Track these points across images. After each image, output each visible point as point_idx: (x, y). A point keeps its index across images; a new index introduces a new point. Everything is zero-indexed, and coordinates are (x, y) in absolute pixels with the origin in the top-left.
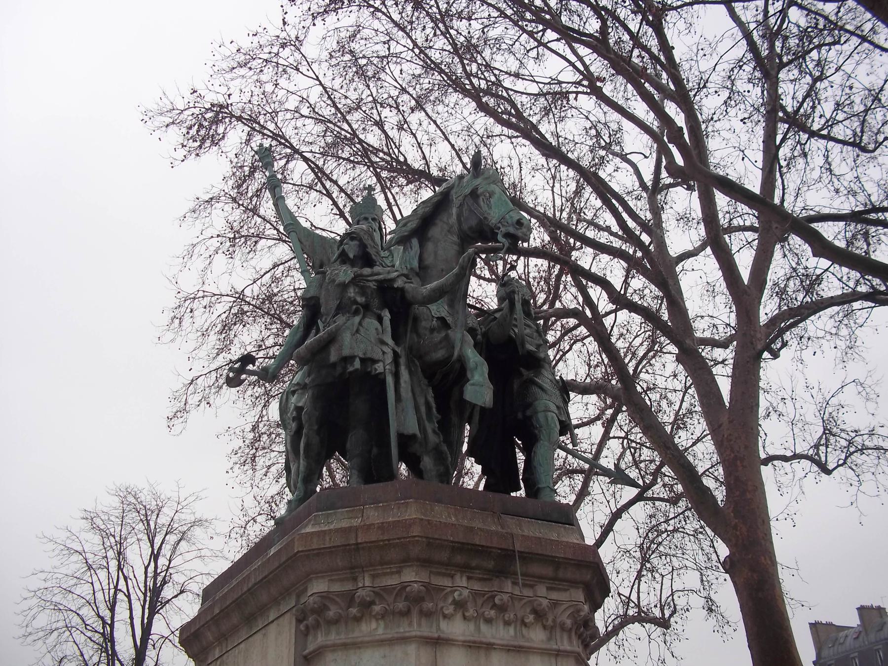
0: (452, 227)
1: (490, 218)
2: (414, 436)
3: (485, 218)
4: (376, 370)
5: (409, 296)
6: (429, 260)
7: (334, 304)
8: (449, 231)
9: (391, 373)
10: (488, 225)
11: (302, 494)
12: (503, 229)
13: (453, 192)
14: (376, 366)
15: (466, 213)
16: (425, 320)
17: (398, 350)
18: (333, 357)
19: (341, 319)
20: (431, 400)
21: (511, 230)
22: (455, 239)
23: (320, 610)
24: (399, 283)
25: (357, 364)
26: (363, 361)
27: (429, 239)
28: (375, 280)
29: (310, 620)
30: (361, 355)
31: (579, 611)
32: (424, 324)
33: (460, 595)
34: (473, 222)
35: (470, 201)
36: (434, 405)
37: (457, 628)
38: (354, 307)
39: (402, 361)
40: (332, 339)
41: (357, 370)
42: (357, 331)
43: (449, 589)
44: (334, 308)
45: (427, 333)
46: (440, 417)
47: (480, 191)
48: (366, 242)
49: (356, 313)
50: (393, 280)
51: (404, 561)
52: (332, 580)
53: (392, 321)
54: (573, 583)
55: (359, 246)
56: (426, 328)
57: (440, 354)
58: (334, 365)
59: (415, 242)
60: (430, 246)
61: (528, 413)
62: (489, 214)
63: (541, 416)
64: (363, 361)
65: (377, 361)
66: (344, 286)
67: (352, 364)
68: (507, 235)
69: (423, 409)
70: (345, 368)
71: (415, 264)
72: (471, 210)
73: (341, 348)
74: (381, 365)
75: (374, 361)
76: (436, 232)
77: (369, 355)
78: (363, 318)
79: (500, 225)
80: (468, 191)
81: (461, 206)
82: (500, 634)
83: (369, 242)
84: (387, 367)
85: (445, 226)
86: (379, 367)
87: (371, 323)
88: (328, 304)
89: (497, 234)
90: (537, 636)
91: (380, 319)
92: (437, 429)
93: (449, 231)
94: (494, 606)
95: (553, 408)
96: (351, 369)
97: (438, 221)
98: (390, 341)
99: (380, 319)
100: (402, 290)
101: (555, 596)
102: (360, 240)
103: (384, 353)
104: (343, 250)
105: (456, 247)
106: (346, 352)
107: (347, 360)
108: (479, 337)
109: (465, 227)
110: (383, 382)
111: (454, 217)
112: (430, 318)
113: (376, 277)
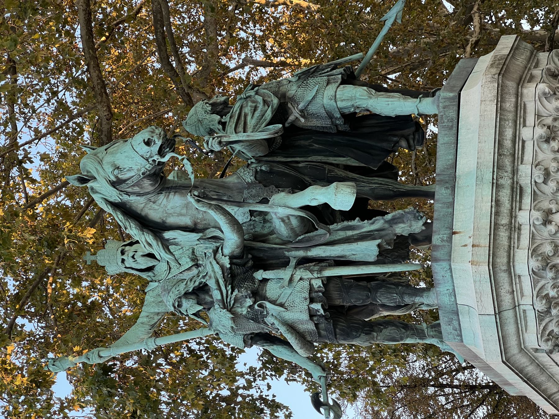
1: (142, 171)
2: (379, 246)
3: (143, 174)
4: (320, 287)
5: (237, 251)
6: (187, 221)
9: (320, 271)
12: (156, 158)
14: (316, 287)
15: (136, 189)
16: (254, 227)
17: (293, 262)
18: (311, 326)
20: (340, 225)
21: (155, 148)
22: (162, 197)
24: (226, 262)
25: (317, 306)
26: (312, 300)
27: (164, 222)
31: (545, 94)
32: (258, 229)
33: (538, 219)
35: (123, 187)
36: (346, 223)
38: (256, 307)
39: (301, 254)
40: (292, 327)
41: (322, 306)
42: (282, 305)
43: (532, 228)
44: (257, 325)
46: (358, 218)
47: (113, 178)
48: (183, 292)
50: (222, 267)
51: (510, 273)
52: (526, 330)
53: (266, 268)
54: (518, 95)
55: (186, 298)
56: (263, 227)
58: (316, 325)
59: (168, 235)
60: (172, 220)
62: (139, 170)
63: (340, 104)
64: (312, 300)
65: (311, 285)
66: (236, 317)
67: (317, 311)
68: (161, 153)
69: (350, 233)
70: (321, 316)
71: (194, 236)
74: (314, 282)
75: (311, 289)
77: (307, 296)
78: (265, 298)
81: (127, 193)
83: (182, 288)
84: (316, 275)
85: (148, 206)
86: (317, 283)
87: (271, 290)
88: (254, 327)
92: (370, 222)
93: (154, 203)
94: (545, 182)
95: (330, 91)
96: (322, 312)
97: (143, 214)
99: (265, 281)
100: (232, 258)
101: (531, 119)
102: (180, 298)
103: (301, 279)
105: (171, 195)
106: (305, 316)
107: (312, 315)
108: (263, 168)
109: (150, 189)
110: (329, 278)
111: (139, 198)
112: (252, 223)
113: (223, 288)
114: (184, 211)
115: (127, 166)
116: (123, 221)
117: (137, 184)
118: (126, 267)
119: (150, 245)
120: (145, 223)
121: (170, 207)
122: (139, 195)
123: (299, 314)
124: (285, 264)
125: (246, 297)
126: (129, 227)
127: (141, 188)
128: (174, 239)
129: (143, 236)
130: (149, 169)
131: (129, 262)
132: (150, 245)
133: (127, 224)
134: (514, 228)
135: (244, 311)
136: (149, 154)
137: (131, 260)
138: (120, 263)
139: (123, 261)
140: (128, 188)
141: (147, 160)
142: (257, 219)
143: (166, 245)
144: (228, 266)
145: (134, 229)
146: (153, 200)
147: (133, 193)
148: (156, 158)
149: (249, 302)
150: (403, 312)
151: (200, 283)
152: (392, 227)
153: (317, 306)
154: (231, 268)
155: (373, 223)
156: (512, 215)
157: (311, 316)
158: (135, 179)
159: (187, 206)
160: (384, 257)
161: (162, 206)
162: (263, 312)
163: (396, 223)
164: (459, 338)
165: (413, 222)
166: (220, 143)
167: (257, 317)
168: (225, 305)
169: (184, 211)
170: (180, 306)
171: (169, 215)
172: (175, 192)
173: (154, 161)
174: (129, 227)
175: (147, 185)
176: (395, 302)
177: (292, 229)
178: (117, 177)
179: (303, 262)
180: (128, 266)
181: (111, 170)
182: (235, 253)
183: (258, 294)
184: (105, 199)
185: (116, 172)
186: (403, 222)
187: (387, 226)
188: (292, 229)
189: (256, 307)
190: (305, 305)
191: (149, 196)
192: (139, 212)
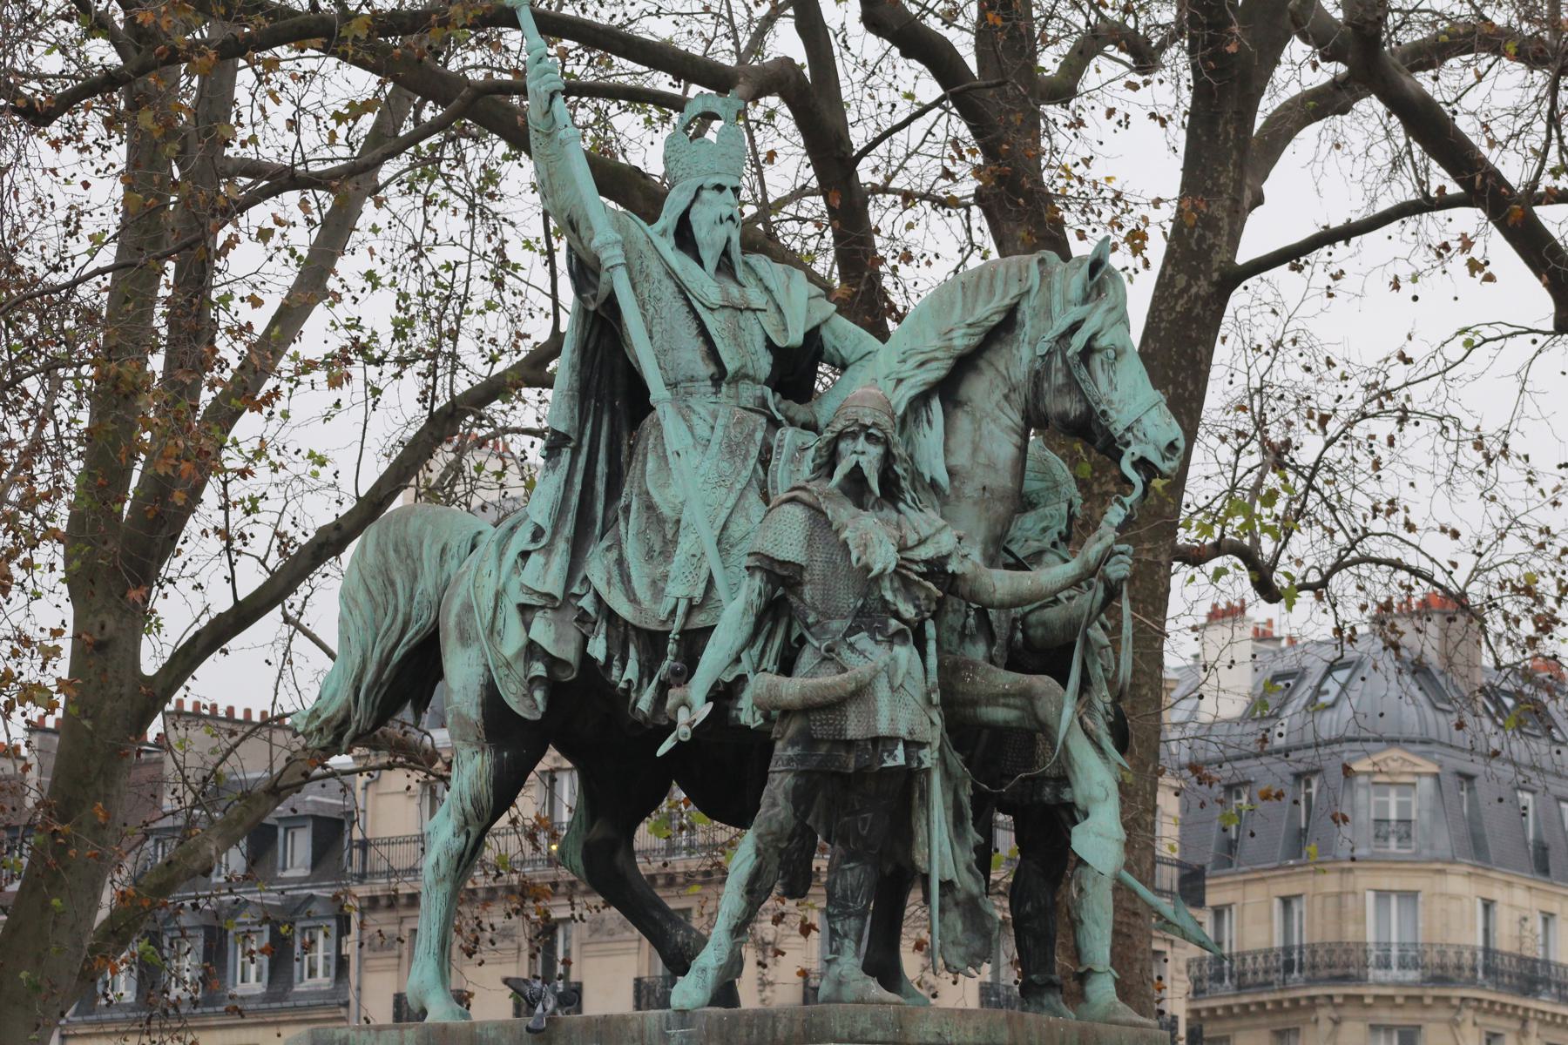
0: (1013, 389)
1: (1112, 413)
3: (1104, 413)
4: (920, 762)
6: (961, 459)
7: (849, 601)
8: (1006, 397)
10: (1106, 430)
11: (725, 958)
12: (1136, 450)
13: (1024, 306)
16: (955, 611)
18: (854, 729)
19: (862, 640)
20: (966, 800)
21: (1154, 457)
22: (1017, 418)
26: (907, 744)
28: (926, 562)
30: (908, 738)
34: (1073, 408)
36: (970, 814)
40: (861, 692)
45: (955, 639)
47: (1102, 342)
48: (895, 451)
49: (900, 635)
50: (949, 556)
56: (952, 629)
57: (999, 714)
58: (850, 744)
59: (936, 404)
61: (1067, 796)
62: (1110, 402)
67: (891, 754)
68: (1142, 464)
69: (950, 819)
72: (1069, 374)
73: (873, 713)
76: (982, 390)
77: (917, 737)
79: (1129, 436)
80: (1078, 342)
85: (999, 381)
89: (1121, 454)
91: (921, 645)
96: (890, 763)
97: (982, 364)
99: (921, 645)
102: (887, 443)
103: (932, 723)
104: (857, 467)
105: (1016, 439)
106: (883, 728)
107: (883, 743)
114: (982, 459)
115: (1118, 379)
116: (987, 324)
117: (1072, 385)
118: (701, 188)
119: (922, 364)
120: (965, 364)
122: (1038, 379)
125: (917, 606)
126: (971, 331)
127: (1059, 390)
128: (929, 422)
129: (947, 354)
130: (1111, 429)
132: (922, 364)
133: (977, 330)
135: (889, 596)
136: (1140, 435)
137: (726, 212)
138: (717, 180)
139: (720, 188)
140: (1065, 361)
141: (1129, 429)
142: (971, 621)
143: (920, 401)
144: (950, 569)
145: (966, 341)
146: (1013, 396)
147: (1048, 367)
148: (1136, 450)
149: (908, 611)
150: (475, 801)
151: (901, 491)
152: (957, 904)
153: (901, 761)
154: (946, 572)
155: (969, 869)
157: (876, 740)
158: (1087, 387)
159: (991, 466)
161: (997, 412)
162: (881, 634)
163: (964, 916)
164: (845, 1035)
165: (962, 950)
166: (1121, 580)
169: (982, 459)
170: (870, 438)
171: (977, 423)
172: (1019, 448)
173: (1128, 444)
174: (971, 331)
176: (844, 897)
177: (975, 703)
178: (1100, 351)
180: (705, 195)
181: (1118, 344)
182: (960, 583)
184: (1028, 292)
185: (1112, 354)
186: (964, 930)
187: (961, 896)
188: (975, 703)
189: (894, 623)
190: (903, 733)
191: (1026, 389)
192: (987, 355)
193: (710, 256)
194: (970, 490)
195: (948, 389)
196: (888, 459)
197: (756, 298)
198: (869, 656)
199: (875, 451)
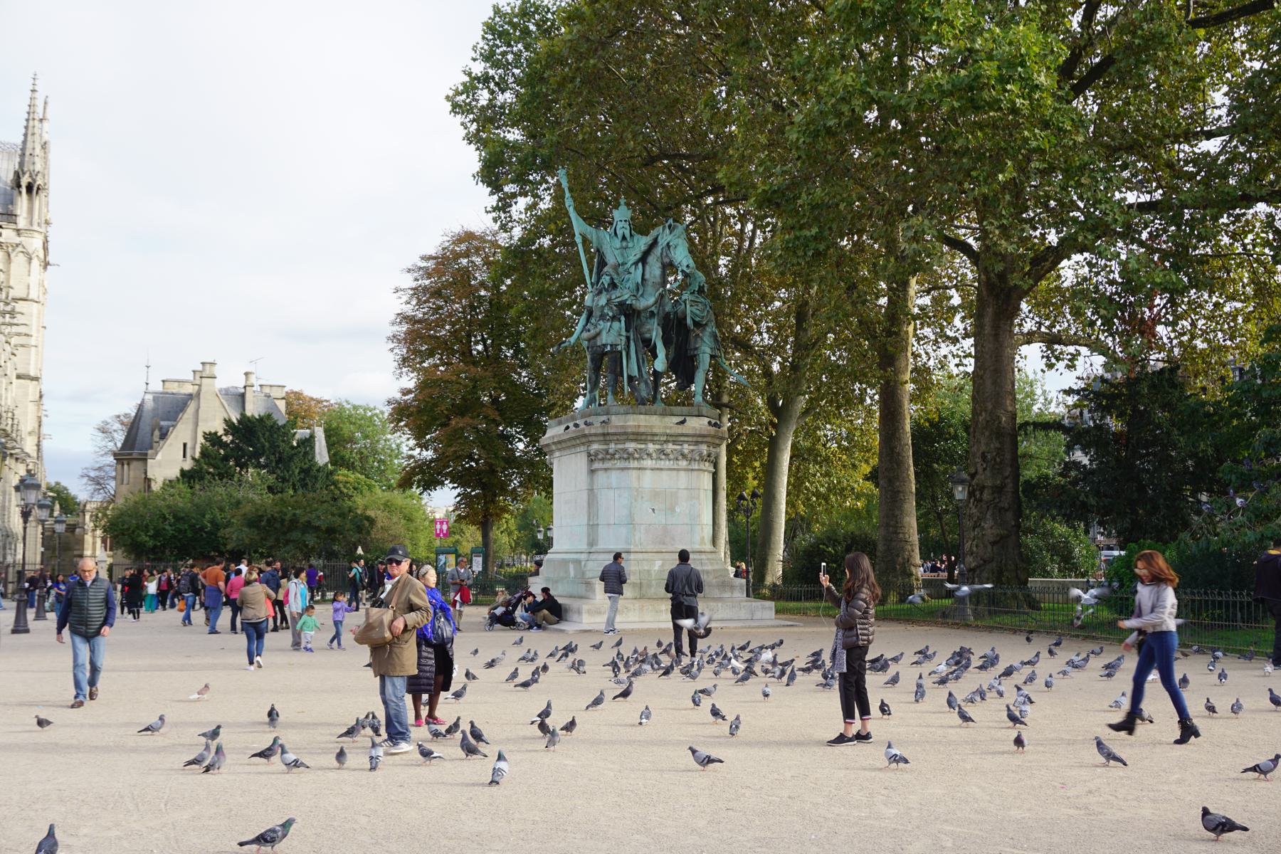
6: (647, 276)
23: (596, 455)
29: (592, 458)
37: (648, 463)
40: (598, 334)
57: (647, 336)
60: (647, 268)
68: (683, 271)
71: (640, 280)
82: (667, 464)
87: (616, 325)
88: (597, 313)
90: (683, 463)
95: (708, 350)
98: (624, 333)
107: (605, 345)
121: (654, 269)
123: (605, 339)
124: (627, 330)
131: (620, 225)
134: (645, 442)
143: (636, 264)
156: (652, 441)
160: (631, 379)
167: (603, 317)
168: (609, 301)
175: (667, 260)
179: (628, 338)
183: (614, 318)
193: (620, 236)
194: (650, 283)
195: (643, 259)
196: (612, 279)
197: (630, 245)
198: (603, 325)
199: (608, 278)
